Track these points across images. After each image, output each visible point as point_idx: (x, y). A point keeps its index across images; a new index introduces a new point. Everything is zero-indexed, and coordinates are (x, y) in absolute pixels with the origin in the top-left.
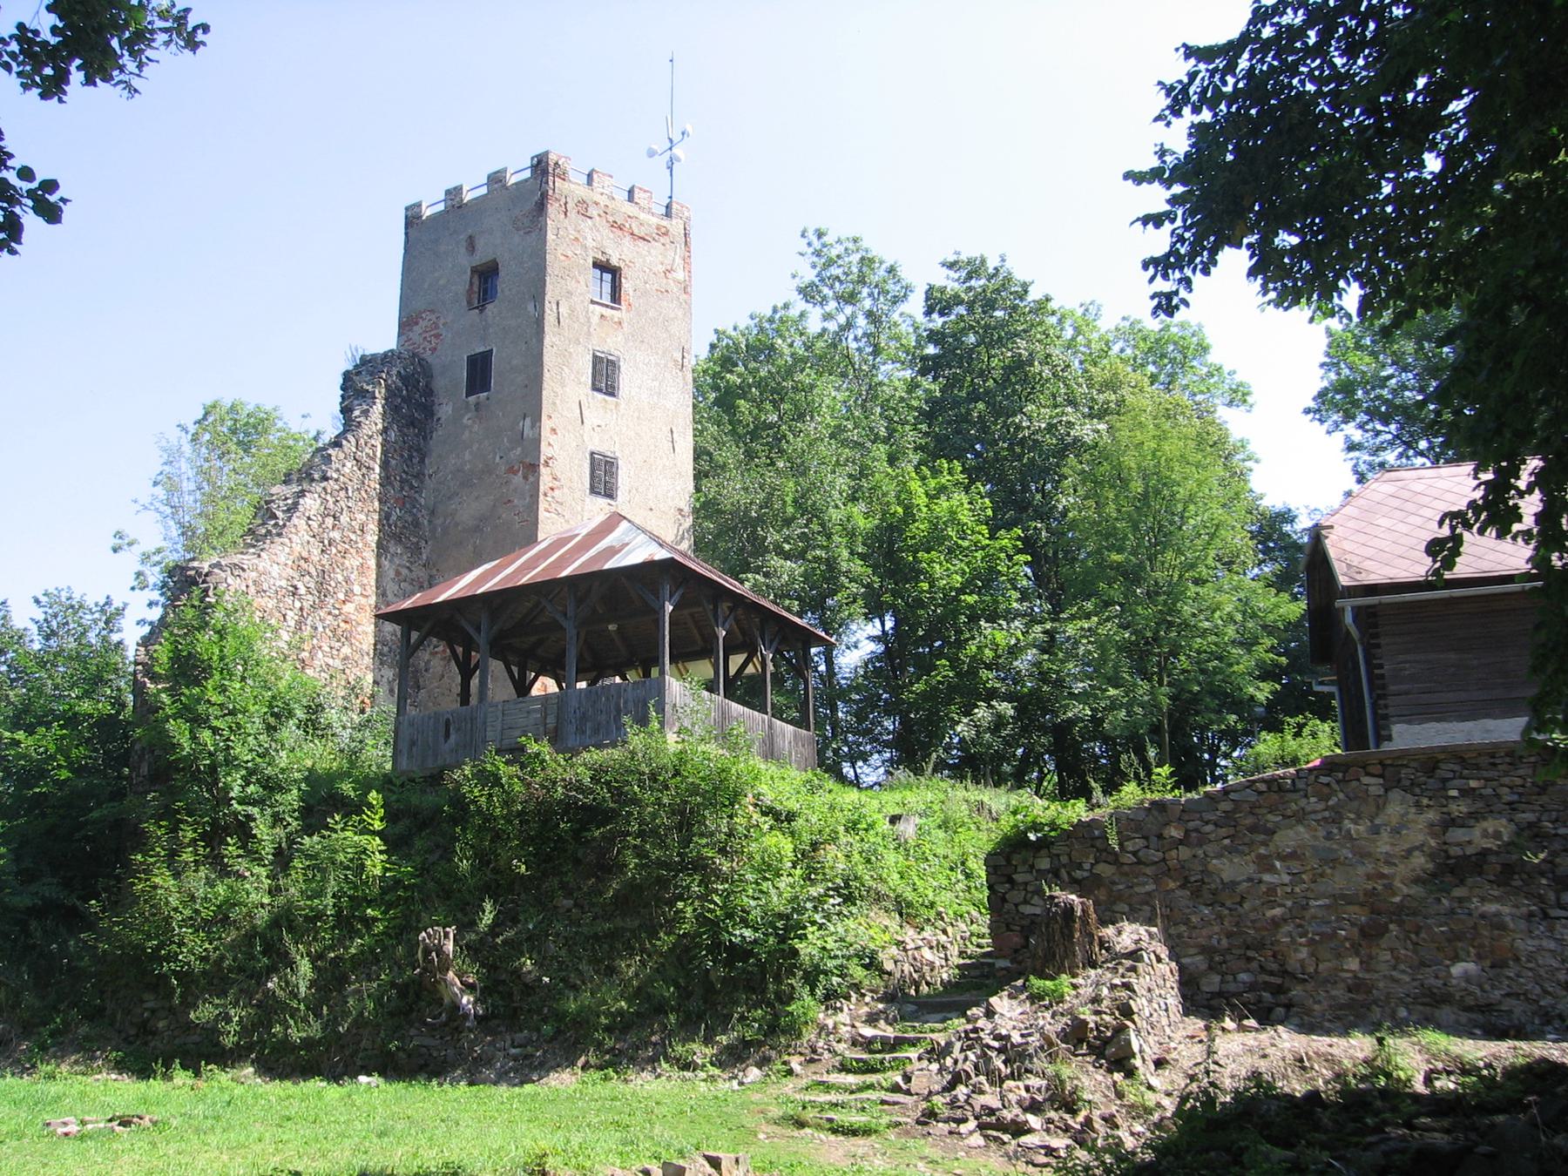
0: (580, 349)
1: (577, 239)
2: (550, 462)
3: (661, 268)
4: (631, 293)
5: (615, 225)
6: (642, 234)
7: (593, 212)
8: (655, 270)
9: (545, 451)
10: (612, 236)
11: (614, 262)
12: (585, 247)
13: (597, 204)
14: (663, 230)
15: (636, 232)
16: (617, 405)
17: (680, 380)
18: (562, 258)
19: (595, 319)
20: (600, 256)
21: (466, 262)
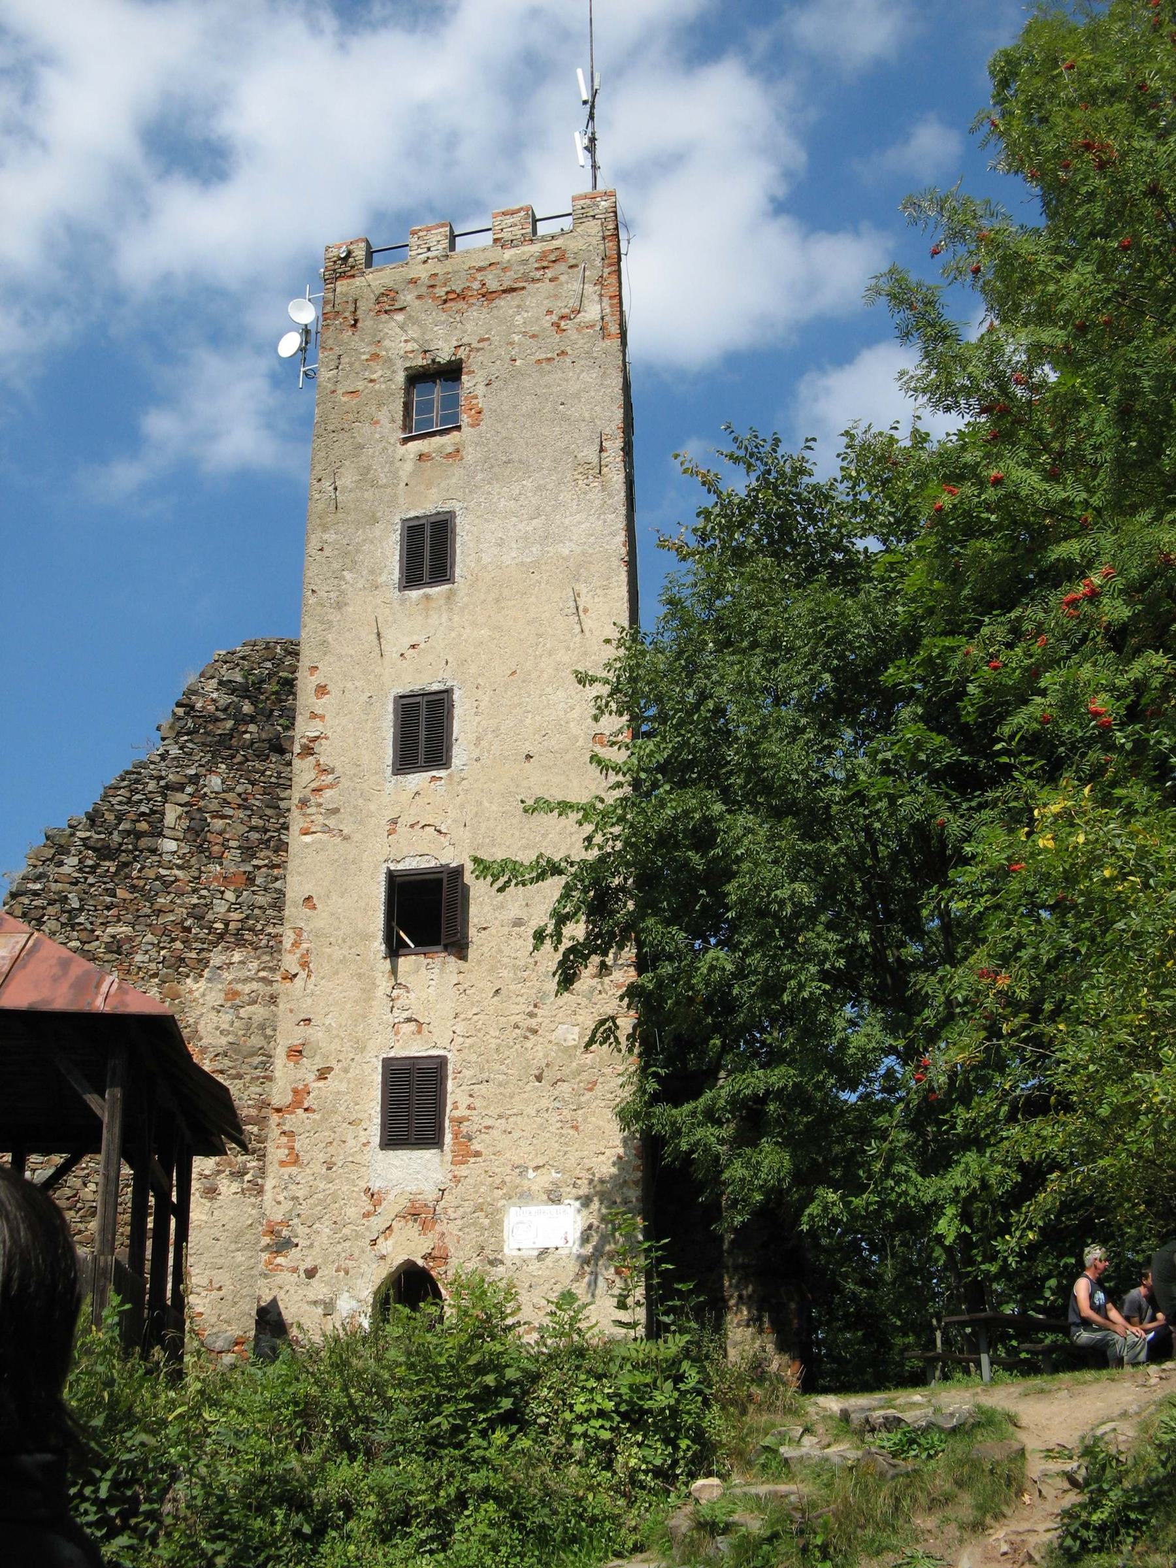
0: (378, 530)
1: (375, 357)
2: (315, 745)
4: (481, 390)
7: (407, 297)
8: (535, 329)
9: (304, 729)
10: (443, 317)
11: (444, 357)
12: (389, 360)
13: (413, 281)
15: (493, 285)
16: (450, 597)
17: (596, 495)
18: (344, 399)
19: (408, 467)
20: (420, 361)
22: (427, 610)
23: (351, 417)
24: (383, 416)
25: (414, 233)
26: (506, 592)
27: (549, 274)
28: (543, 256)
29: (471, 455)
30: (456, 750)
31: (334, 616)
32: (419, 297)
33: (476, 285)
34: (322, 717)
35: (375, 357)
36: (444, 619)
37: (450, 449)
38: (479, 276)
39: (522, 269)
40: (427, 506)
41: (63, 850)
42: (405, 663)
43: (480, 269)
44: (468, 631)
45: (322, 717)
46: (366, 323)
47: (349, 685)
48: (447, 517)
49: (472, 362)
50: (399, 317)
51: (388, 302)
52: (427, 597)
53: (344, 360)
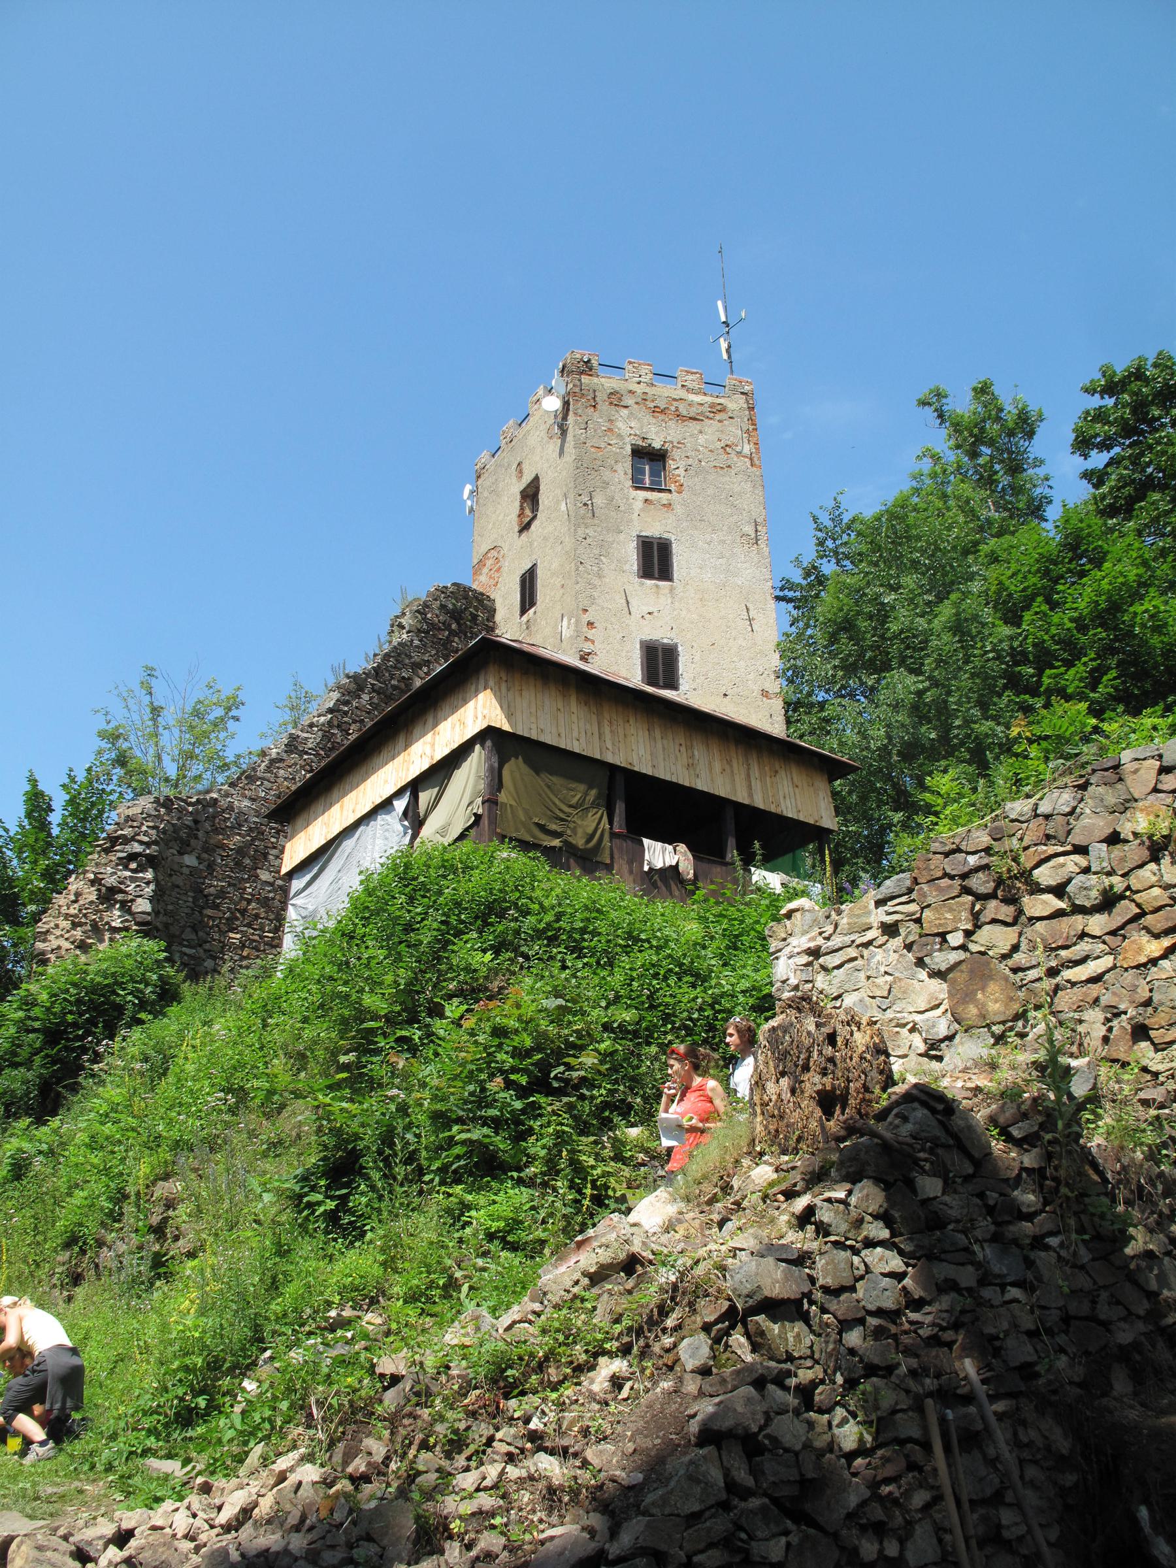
0: (622, 537)
1: (610, 430)
3: (719, 445)
5: (656, 411)
6: (692, 415)
8: (712, 447)
10: (654, 421)
11: (657, 445)
12: (620, 436)
14: (719, 408)
15: (685, 413)
16: (672, 589)
19: (638, 505)
21: (517, 487)
22: (658, 593)
23: (599, 463)
24: (619, 467)
25: (630, 363)
26: (706, 596)
27: (718, 417)
28: (712, 405)
29: (679, 509)
30: (681, 681)
31: (596, 581)
32: (637, 403)
33: (673, 409)
34: (593, 642)
35: (610, 430)
36: (669, 601)
37: (665, 502)
38: (676, 404)
39: (701, 409)
40: (654, 530)
41: (361, 688)
42: (645, 622)
43: (675, 400)
44: (684, 613)
45: (593, 642)
46: (603, 406)
47: (609, 626)
48: (643, 542)
49: (675, 454)
50: (625, 412)
51: (616, 400)
52: (657, 586)
53: (590, 425)
